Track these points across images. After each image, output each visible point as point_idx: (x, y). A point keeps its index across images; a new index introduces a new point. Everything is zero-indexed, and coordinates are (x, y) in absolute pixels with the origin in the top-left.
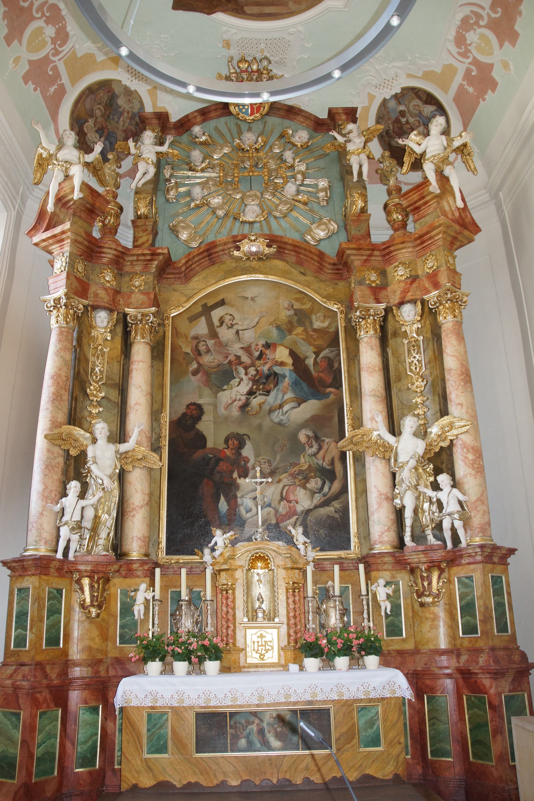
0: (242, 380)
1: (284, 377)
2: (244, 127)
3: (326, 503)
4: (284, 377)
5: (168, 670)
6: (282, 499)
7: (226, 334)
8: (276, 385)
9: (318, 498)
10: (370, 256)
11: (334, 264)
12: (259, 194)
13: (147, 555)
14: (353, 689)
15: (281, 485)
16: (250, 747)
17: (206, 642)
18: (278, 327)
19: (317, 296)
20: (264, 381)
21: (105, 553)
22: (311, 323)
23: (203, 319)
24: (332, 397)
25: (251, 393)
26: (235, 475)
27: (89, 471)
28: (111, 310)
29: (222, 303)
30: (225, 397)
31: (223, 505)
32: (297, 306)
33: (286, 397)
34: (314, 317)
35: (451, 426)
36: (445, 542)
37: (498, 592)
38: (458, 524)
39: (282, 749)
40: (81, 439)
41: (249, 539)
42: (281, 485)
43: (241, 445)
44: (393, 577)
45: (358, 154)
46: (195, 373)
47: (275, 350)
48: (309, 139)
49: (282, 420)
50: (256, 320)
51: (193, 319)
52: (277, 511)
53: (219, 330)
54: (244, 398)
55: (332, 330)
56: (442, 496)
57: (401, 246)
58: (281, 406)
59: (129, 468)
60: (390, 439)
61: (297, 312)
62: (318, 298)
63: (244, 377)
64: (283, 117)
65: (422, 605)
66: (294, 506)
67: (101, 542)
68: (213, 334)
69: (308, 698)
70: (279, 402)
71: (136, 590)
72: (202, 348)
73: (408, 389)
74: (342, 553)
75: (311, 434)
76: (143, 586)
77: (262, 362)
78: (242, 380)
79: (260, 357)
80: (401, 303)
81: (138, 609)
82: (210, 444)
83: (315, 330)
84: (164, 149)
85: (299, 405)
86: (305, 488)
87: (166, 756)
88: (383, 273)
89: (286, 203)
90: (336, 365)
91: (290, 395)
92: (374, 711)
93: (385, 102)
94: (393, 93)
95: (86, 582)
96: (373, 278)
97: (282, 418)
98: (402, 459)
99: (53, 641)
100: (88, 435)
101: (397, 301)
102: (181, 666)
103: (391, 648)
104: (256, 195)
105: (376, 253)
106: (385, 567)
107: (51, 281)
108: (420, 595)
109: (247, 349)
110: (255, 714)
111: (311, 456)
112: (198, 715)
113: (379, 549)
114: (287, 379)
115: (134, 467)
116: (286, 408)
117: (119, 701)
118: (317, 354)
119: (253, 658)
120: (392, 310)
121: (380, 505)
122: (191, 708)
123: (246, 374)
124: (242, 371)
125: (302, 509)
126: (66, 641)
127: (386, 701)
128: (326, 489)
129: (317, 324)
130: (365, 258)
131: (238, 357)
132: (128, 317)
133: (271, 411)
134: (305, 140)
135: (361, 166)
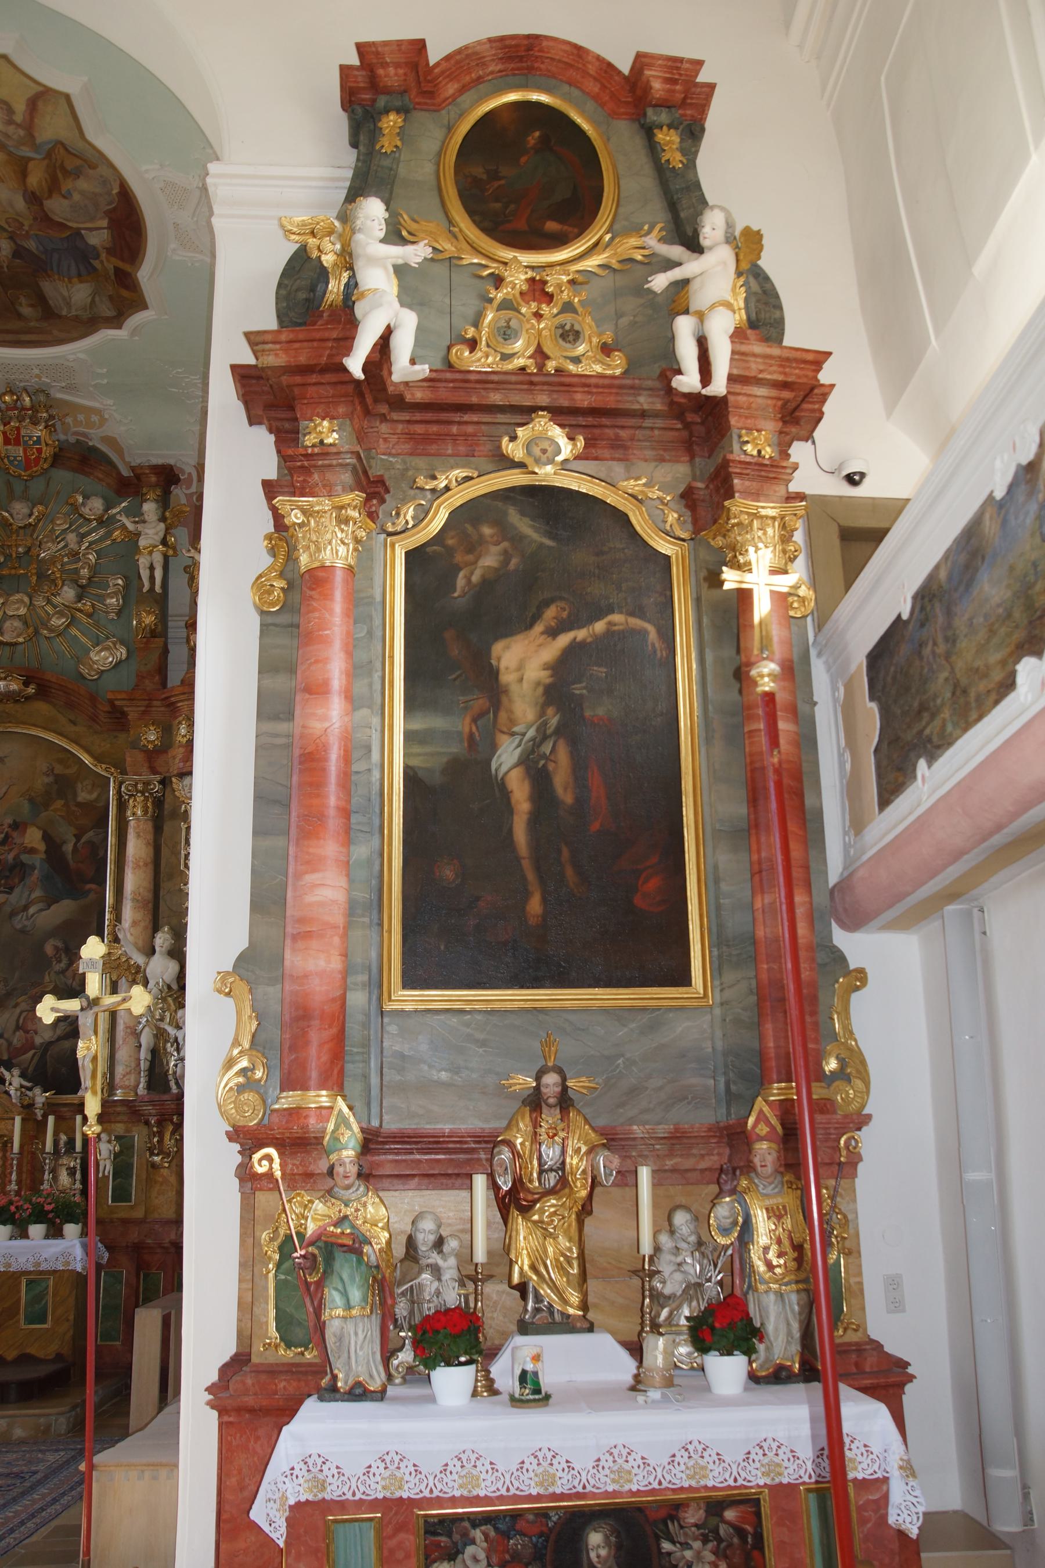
1: (33, 868)
2: (18, 487)
4: (33, 868)
6: (18, 1028)
8: (22, 879)
10: (147, 707)
11: (109, 712)
12: (26, 599)
14: (22, 1260)
15: (18, 1011)
18: (31, 800)
19: (86, 755)
20: (7, 874)
22: (75, 795)
24: (92, 896)
32: (59, 769)
33: (33, 896)
34: (79, 785)
42: (18, 1011)
44: (128, 1130)
45: (151, 553)
47: (24, 832)
48: (106, 510)
49: (25, 926)
50: (4, 790)
52: (10, 1044)
55: (101, 804)
57: (182, 697)
58: (26, 908)
60: (139, 959)
61: (59, 779)
62: (87, 760)
64: (75, 470)
65: (154, 1165)
66: (32, 1038)
70: (23, 902)
75: (60, 944)
77: (6, 848)
83: (79, 805)
85: (49, 906)
89: (61, 614)
90: (101, 854)
91: (37, 893)
92: (44, 1285)
96: (152, 738)
97: (26, 923)
101: (175, 772)
103: (116, 1216)
104: (22, 601)
105: (155, 703)
106: (119, 1118)
111: (58, 973)
114: (36, 872)
116: (32, 911)
118: (78, 837)
120: (171, 782)
121: (124, 1040)
125: (42, 1041)
127: (58, 1275)
129: (83, 796)
130: (143, 709)
133: (13, 914)
134: (100, 512)
135: (152, 568)
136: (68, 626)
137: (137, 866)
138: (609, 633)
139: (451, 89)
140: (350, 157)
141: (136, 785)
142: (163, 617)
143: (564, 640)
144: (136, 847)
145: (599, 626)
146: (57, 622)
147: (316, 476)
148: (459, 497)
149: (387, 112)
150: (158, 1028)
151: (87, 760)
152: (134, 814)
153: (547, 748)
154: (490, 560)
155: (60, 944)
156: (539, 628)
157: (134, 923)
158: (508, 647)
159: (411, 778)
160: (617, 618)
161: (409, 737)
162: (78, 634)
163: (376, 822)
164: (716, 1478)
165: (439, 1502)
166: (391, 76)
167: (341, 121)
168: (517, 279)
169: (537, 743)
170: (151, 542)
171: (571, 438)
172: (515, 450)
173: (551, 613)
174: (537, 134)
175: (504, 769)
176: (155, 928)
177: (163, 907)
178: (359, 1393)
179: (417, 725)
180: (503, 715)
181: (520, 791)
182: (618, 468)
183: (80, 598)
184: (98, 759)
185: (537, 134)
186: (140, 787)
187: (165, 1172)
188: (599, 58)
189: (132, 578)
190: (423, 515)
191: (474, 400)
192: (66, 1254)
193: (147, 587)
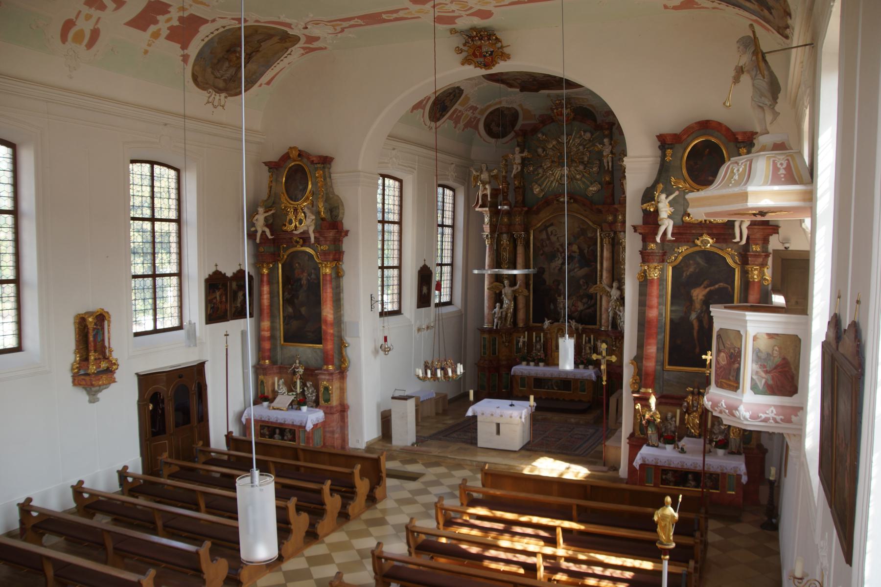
0: (559, 258)
3: (588, 308)
5: (528, 364)
6: (573, 305)
7: (554, 239)
9: (586, 306)
13: (524, 325)
16: (548, 389)
17: (539, 357)
21: (509, 326)
26: (556, 296)
27: (503, 298)
28: (507, 233)
29: (552, 225)
30: (553, 265)
31: (552, 307)
39: (558, 390)
40: (500, 287)
41: (559, 322)
42: (573, 301)
43: (559, 285)
45: (607, 157)
46: (542, 255)
48: (591, 137)
51: (541, 231)
53: (551, 237)
54: (560, 266)
58: (574, 270)
59: (518, 295)
60: (608, 289)
62: (591, 224)
63: (560, 257)
65: (613, 350)
67: (508, 322)
68: (549, 239)
69: (565, 377)
71: (520, 337)
72: (545, 244)
73: (621, 267)
74: (594, 327)
75: (585, 281)
76: (522, 337)
81: (521, 344)
82: (547, 283)
84: (525, 154)
85: (581, 269)
86: (581, 301)
87: (525, 389)
88: (615, 217)
89: (579, 174)
91: (577, 265)
95: (504, 335)
98: (612, 298)
99: (494, 353)
100: (502, 285)
102: (532, 364)
107: (484, 226)
108: (613, 347)
110: (550, 380)
112: (535, 379)
115: (519, 295)
116: (576, 270)
117: (512, 373)
118: (589, 248)
122: (533, 376)
123: (561, 256)
124: (559, 255)
126: (498, 352)
128: (589, 302)
129: (589, 235)
131: (558, 249)
132: (515, 236)
136: (582, 178)
137: (607, 260)
138: (720, 289)
139: (685, 137)
140: (659, 153)
141: (606, 234)
142: (612, 178)
143: (708, 289)
145: (717, 286)
147: (650, 257)
148: (684, 254)
149: (668, 149)
150: (615, 311)
151: (591, 224)
152: (606, 243)
153: (702, 315)
154: (691, 270)
155: (585, 281)
156: (702, 286)
157: (607, 277)
158: (695, 291)
159: (671, 320)
160: (722, 284)
161: (671, 311)
162: (585, 180)
163: (663, 330)
165: (664, 467)
166: (669, 141)
169: (700, 313)
170: (607, 153)
171: (712, 239)
172: (698, 242)
173: (706, 283)
174: (708, 150)
175: (693, 319)
176: (613, 281)
177: (615, 273)
178: (653, 446)
179: (674, 308)
180: (693, 307)
181: (696, 324)
182: (724, 245)
183: (585, 169)
184: (594, 223)
185: (708, 150)
186: (607, 235)
187: (617, 352)
188: (725, 126)
189: (601, 161)
190: (676, 258)
191: (688, 232)
192: (590, 375)
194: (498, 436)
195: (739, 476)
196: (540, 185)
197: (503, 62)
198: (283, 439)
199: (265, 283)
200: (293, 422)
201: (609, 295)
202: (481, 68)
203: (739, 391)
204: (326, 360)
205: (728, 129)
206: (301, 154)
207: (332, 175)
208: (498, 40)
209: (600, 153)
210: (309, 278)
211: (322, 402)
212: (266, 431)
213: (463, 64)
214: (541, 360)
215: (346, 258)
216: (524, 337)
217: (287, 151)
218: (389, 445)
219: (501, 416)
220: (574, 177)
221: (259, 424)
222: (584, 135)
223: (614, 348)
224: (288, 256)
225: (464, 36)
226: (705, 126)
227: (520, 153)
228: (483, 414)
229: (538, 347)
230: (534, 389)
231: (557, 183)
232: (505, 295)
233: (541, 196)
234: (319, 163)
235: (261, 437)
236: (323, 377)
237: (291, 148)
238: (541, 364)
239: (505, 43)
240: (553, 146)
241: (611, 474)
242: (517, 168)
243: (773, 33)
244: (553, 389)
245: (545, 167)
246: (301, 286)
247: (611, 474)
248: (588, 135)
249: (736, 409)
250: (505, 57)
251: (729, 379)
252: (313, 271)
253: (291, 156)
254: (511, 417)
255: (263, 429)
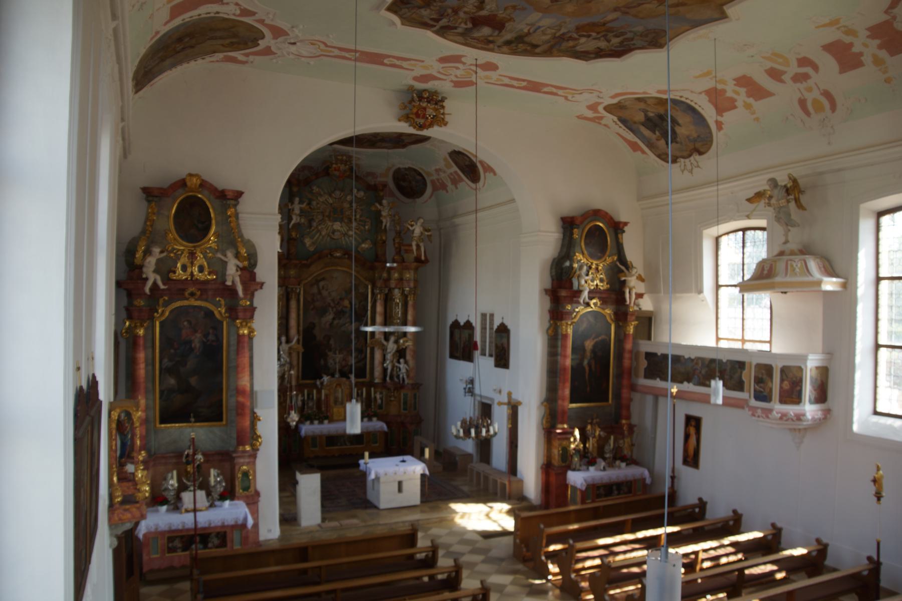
5: (312, 423)
7: (325, 293)
12: (340, 225)
23: (316, 286)
25: (334, 319)
29: (323, 279)
31: (322, 362)
35: (407, 341)
36: (400, 380)
37: (415, 398)
38: (405, 377)
56: (402, 366)
58: (345, 324)
59: (292, 352)
60: (385, 343)
65: (391, 401)
68: (320, 293)
78: (330, 313)
79: (338, 303)
80: (394, 289)
93: (399, 169)
94: (404, 167)
98: (389, 350)
108: (390, 397)
109: (333, 300)
113: (377, 381)
116: (347, 325)
119: (335, 418)
123: (332, 310)
124: (330, 309)
135: (386, 223)
141: (381, 290)
143: (595, 340)
144: (379, 308)
146: (350, 233)
149: (575, 228)
164: (629, 479)
166: (577, 222)
167: (561, 223)
168: (594, 267)
171: (600, 301)
181: (587, 369)
193: (383, 227)
194: (401, 495)
195: (644, 480)
196: (312, 238)
197: (439, 127)
198: (206, 547)
199: (141, 348)
200: (223, 523)
201: (384, 349)
202: (415, 127)
203: (802, 404)
204: (241, 441)
205: (611, 218)
206: (204, 185)
207: (240, 215)
208: (443, 107)
209: (380, 211)
210: (204, 340)
211: (239, 490)
212: (177, 543)
213: (400, 120)
214: (326, 418)
215: (257, 314)
216: (303, 395)
217: (184, 177)
218: (298, 528)
219: (405, 473)
220: (346, 234)
221: (167, 535)
222: (357, 193)
223: (392, 399)
224: (171, 312)
225: (415, 95)
226: (597, 214)
227: (299, 203)
228: (386, 474)
229: (311, 404)
230: (327, 448)
231: (329, 238)
232: (283, 353)
233: (312, 249)
234: (232, 199)
235: (169, 552)
236: (242, 460)
237: (191, 175)
238: (326, 422)
239: (446, 111)
240: (326, 200)
241: (524, 504)
242: (297, 219)
243: (643, 152)
244: (346, 445)
245: (317, 221)
246: (191, 350)
247: (524, 504)
248: (362, 194)
249: (804, 415)
250: (443, 123)
251: (792, 398)
252: (211, 331)
253: (188, 184)
254: (414, 472)
255: (172, 542)
